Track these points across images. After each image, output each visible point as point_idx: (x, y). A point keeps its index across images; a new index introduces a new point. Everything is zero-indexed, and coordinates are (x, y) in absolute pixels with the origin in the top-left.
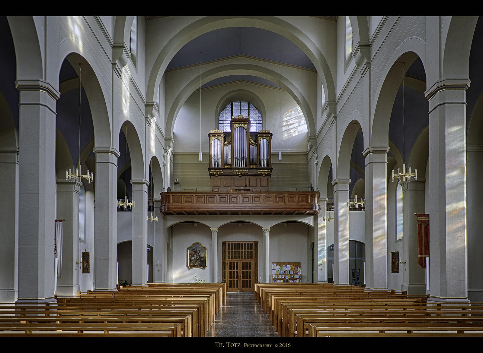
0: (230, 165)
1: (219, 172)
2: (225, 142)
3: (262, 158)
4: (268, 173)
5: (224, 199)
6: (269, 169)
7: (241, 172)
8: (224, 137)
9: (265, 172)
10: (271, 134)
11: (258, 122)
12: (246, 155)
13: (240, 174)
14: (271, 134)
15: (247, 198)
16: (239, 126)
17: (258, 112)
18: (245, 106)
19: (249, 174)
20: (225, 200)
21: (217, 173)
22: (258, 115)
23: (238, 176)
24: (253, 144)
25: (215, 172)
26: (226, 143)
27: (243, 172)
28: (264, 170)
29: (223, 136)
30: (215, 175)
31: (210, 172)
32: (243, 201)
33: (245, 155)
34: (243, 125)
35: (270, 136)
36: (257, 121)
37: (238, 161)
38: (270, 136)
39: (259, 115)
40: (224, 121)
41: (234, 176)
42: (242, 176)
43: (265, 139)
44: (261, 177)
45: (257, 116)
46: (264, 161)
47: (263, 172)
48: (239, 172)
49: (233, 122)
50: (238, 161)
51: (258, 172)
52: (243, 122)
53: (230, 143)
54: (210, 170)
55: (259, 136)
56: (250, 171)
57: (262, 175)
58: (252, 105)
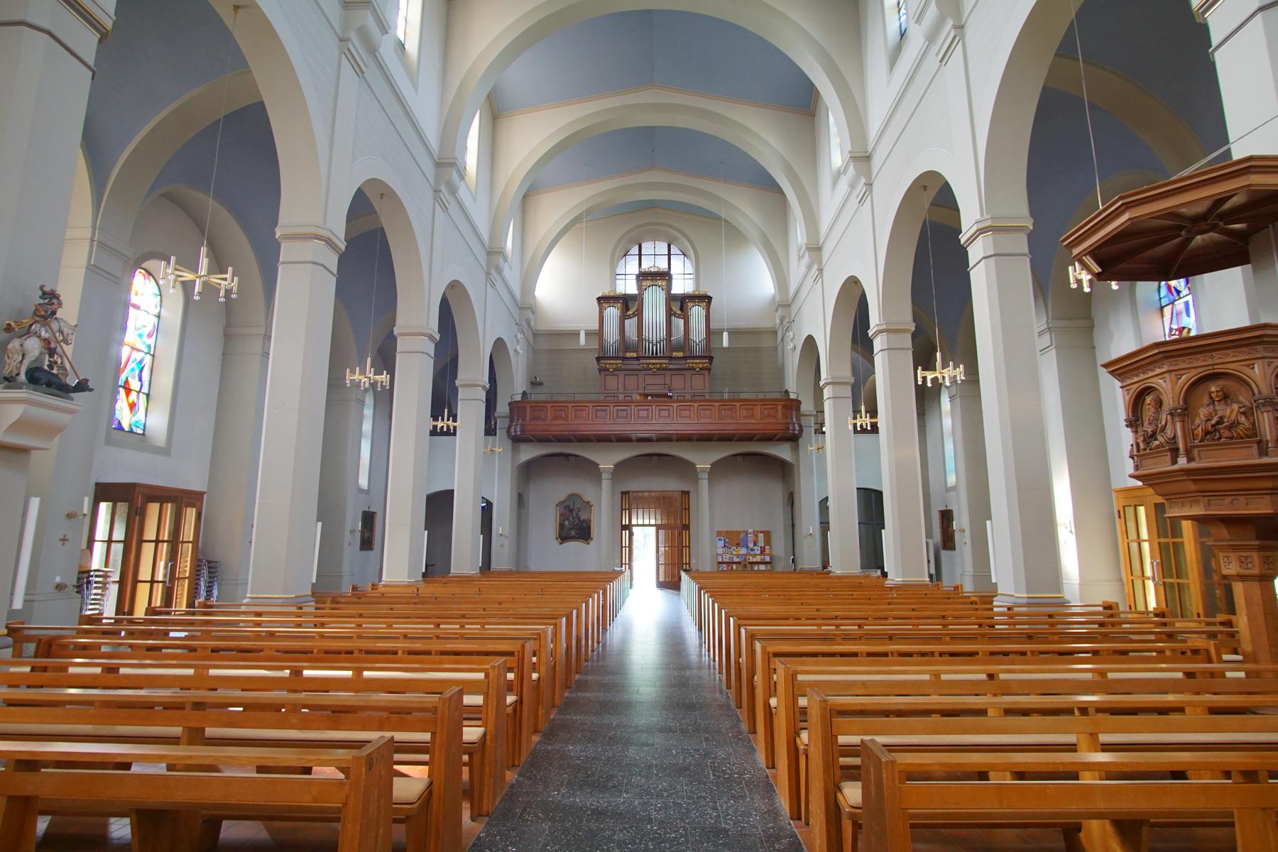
1: (616, 364)
2: (626, 312)
10: (710, 298)
11: (687, 276)
13: (654, 368)
14: (710, 298)
16: (652, 283)
18: (663, 250)
19: (671, 367)
27: (661, 364)
28: (698, 361)
30: (608, 370)
32: (660, 417)
33: (663, 334)
34: (660, 283)
37: (651, 345)
44: (693, 372)
47: (696, 363)
48: (653, 364)
50: (651, 345)
56: (672, 362)
57: (694, 369)
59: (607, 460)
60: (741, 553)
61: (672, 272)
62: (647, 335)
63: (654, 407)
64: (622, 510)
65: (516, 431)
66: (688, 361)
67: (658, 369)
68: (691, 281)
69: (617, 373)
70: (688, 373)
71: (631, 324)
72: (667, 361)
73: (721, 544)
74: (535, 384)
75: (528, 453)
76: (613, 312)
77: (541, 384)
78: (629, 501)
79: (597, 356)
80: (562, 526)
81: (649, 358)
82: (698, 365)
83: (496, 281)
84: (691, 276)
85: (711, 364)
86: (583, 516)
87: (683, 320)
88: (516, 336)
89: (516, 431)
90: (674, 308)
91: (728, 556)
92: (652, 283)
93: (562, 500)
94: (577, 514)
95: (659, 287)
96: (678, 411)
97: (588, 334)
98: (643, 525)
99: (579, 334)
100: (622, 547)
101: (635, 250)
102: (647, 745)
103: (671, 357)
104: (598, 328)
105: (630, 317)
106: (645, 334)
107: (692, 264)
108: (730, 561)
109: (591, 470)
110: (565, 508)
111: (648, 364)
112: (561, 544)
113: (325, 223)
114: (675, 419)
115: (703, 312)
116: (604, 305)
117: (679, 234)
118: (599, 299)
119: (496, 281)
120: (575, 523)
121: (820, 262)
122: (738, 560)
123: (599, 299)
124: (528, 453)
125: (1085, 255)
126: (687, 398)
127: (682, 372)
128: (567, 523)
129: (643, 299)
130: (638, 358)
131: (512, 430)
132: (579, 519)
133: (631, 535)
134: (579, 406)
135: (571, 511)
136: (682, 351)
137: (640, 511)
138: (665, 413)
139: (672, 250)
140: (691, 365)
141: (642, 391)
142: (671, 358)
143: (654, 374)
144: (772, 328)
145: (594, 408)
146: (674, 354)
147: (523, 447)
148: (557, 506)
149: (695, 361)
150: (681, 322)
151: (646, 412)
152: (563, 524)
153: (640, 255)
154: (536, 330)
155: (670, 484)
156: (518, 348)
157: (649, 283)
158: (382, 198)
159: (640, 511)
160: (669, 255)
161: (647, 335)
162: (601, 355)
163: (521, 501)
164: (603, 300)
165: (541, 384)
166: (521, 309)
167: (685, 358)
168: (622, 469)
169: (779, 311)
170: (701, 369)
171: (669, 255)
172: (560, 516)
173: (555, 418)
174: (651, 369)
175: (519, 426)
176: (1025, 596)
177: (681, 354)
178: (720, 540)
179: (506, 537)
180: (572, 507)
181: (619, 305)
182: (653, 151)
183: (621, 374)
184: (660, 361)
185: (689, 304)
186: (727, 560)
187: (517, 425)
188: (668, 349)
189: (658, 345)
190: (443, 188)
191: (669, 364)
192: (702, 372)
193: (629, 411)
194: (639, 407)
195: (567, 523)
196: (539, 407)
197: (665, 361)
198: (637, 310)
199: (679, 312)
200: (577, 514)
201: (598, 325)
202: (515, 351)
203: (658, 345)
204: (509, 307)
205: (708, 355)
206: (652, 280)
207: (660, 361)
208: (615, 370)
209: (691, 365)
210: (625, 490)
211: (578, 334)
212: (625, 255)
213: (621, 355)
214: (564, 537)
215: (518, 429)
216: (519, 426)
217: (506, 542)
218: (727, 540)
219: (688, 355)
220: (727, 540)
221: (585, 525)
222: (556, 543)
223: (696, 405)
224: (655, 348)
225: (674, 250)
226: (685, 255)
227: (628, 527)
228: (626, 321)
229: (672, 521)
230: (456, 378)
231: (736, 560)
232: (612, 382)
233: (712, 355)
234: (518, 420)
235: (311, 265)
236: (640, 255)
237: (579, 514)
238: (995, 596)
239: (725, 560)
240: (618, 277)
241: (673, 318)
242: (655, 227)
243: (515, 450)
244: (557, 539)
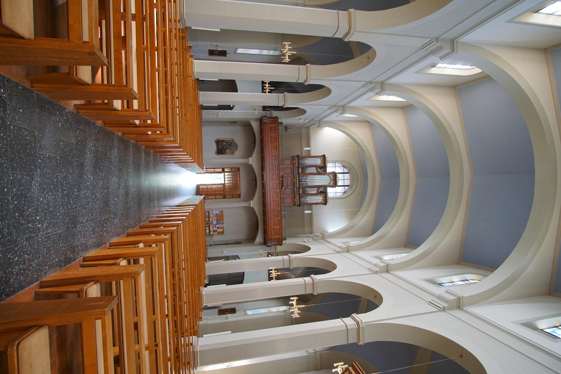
2: (319, 168)
4: (296, 203)
5: (275, 168)
7: (296, 181)
9: (297, 200)
10: (326, 204)
14: (326, 204)
15: (275, 187)
16: (332, 179)
19: (295, 188)
20: (274, 169)
25: (296, 161)
26: (318, 169)
27: (296, 183)
28: (298, 200)
30: (293, 160)
32: (273, 184)
33: (310, 184)
44: (293, 198)
47: (297, 199)
48: (296, 180)
57: (295, 199)
58: (348, 188)
59: (253, 161)
60: (214, 221)
62: (309, 177)
63: (277, 181)
64: (231, 168)
65: (265, 120)
66: (298, 196)
67: (294, 182)
68: (333, 196)
70: (292, 196)
71: (313, 170)
72: (298, 186)
73: (218, 213)
74: (286, 128)
75: (255, 125)
76: (319, 162)
77: (286, 131)
78: (235, 171)
79: (299, 155)
80: (223, 141)
81: (299, 178)
82: (296, 200)
83: (331, 110)
84: (335, 196)
85: (297, 206)
86: (228, 151)
88: (307, 119)
89: (265, 120)
90: (321, 189)
91: (212, 216)
92: (332, 179)
93: (235, 141)
94: (228, 148)
95: (330, 182)
96: (276, 192)
97: (309, 151)
98: (225, 178)
99: (309, 147)
100: (214, 169)
101: (346, 171)
102: (119, 187)
103: (299, 188)
104: (311, 155)
105: (317, 169)
106: (309, 177)
107: (340, 196)
108: (210, 217)
109: (249, 154)
110: (231, 143)
112: (215, 141)
113: (356, 31)
114: (272, 191)
115: (319, 202)
116: (322, 158)
117: (353, 189)
118: (324, 156)
119: (331, 110)
120: (224, 147)
121: (342, 252)
122: (210, 220)
123: (324, 156)
124: (255, 125)
125: (349, 372)
126: (282, 196)
127: (293, 194)
128: (225, 143)
129: (325, 175)
130: (299, 173)
131: (265, 118)
132: (226, 149)
133: (220, 172)
134: (277, 148)
135: (230, 145)
136: (302, 192)
137: (231, 176)
138: (275, 187)
139: (346, 187)
140: (296, 197)
141: (284, 176)
142: (299, 188)
143: (292, 181)
144: (313, 232)
145: (276, 155)
146: (301, 190)
147: (258, 123)
148: (232, 139)
150: (315, 192)
151: (275, 178)
152: (224, 142)
153: (344, 173)
154: (310, 128)
155: (243, 189)
156: (302, 120)
157: (332, 177)
158: (367, 58)
159: (231, 176)
160: (344, 186)
161: (309, 177)
162: (299, 157)
163: (234, 123)
164: (324, 157)
165: (286, 131)
166: (319, 121)
167: (299, 194)
168: (250, 168)
169: (321, 235)
171: (344, 186)
172: (227, 140)
173: (271, 137)
174: (294, 179)
175: (267, 121)
176: (198, 350)
177: (301, 192)
178: (219, 212)
179: (217, 116)
180: (232, 145)
181: (322, 165)
182: (389, 178)
183: (291, 166)
184: (298, 183)
186: (210, 216)
187: (267, 120)
188: (304, 187)
189: (305, 182)
190: (372, 85)
191: (296, 188)
192: (293, 202)
193: (275, 170)
194: (277, 174)
195: (225, 143)
196: (276, 130)
198: (320, 172)
199: (319, 191)
200: (228, 148)
201: (313, 155)
202: (301, 119)
203: (305, 182)
204: (320, 115)
205: (301, 205)
206: (333, 179)
207: (298, 183)
208: (293, 163)
209: (296, 197)
210: (240, 169)
211: (309, 146)
212: (344, 167)
213: (300, 166)
214: (218, 142)
215: (266, 121)
216: (267, 121)
217: (215, 116)
218: (219, 215)
219: (301, 195)
220: (219, 215)
221: (224, 152)
222: (215, 139)
223: (279, 200)
224: (303, 181)
225: (346, 188)
226: (344, 193)
227: (223, 171)
229: (227, 190)
230: (288, 92)
231: (211, 219)
232: (288, 162)
233: (301, 206)
234: (270, 121)
235: (337, 25)
236: (344, 173)
237: (229, 149)
238: (197, 336)
239: (210, 215)
240: (334, 164)
241: (317, 188)
242: (356, 179)
243: (256, 120)
244: (217, 139)
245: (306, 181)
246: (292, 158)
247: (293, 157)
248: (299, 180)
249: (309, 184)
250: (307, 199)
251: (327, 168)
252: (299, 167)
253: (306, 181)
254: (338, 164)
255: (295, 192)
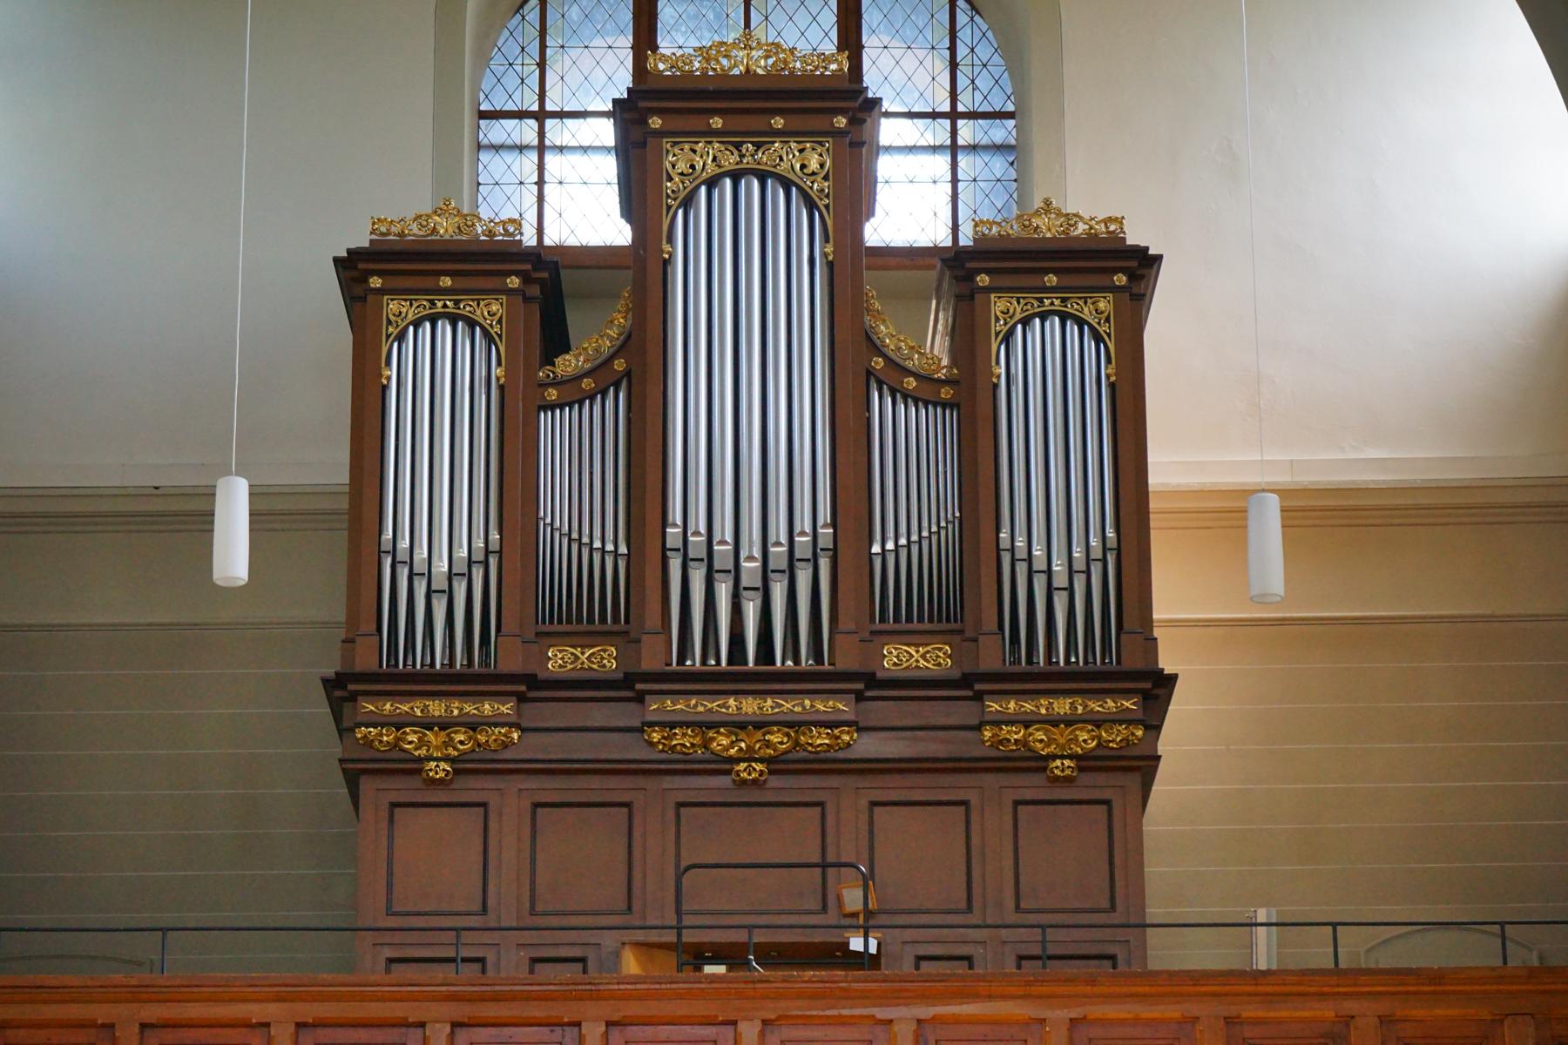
0: (624, 635)
1: (473, 726)
2: (548, 360)
3: (1038, 552)
4: (1115, 736)
6: (1127, 693)
7: (761, 725)
8: (535, 290)
10: (1143, 264)
12: (824, 513)
14: (1143, 264)
16: (730, 160)
17: (962, 18)
19: (869, 746)
21: (449, 743)
22: (962, 51)
23: (724, 781)
24: (911, 383)
26: (567, 364)
27: (793, 725)
28: (1062, 706)
29: (526, 279)
30: (412, 767)
31: (344, 731)
34: (788, 156)
35: (1121, 279)
36: (953, 115)
37: (723, 592)
38: (1121, 279)
39: (984, 52)
40: (541, 116)
41: (668, 782)
42: (774, 782)
43: (1064, 318)
44: (1030, 785)
45: (954, 66)
46: (1060, 580)
47: (1053, 722)
48: (739, 726)
49: (656, 122)
50: (723, 592)
51: (978, 728)
52: (778, 122)
53: (619, 365)
54: (353, 697)
55: (983, 280)
56: (881, 711)
57: (1036, 763)
61: (872, 81)
67: (778, 765)
69: (472, 789)
72: (842, 707)
79: (330, 672)
82: (1061, 735)
87: (951, 417)
95: (787, 184)
105: (573, 395)
111: (706, 726)
140: (1016, 734)
142: (868, 684)
143: (749, 799)
146: (897, 657)
149: (1042, 706)
157: (707, 156)
162: (366, 661)
170: (1087, 762)
174: (722, 766)
184: (791, 706)
185: (999, 304)
197: (823, 706)
205: (1132, 662)
208: (463, 767)
209: (1016, 734)
213: (510, 659)
219: (991, 657)
228: (544, 419)
233: (1167, 664)
245: (751, 567)
246: (367, 785)
247: (352, 780)
248: (735, 680)
249: (804, 522)
250: (1058, 567)
251: (560, 249)
252: (532, 681)
253: (751, 567)
254: (497, 62)
255: (930, 746)
